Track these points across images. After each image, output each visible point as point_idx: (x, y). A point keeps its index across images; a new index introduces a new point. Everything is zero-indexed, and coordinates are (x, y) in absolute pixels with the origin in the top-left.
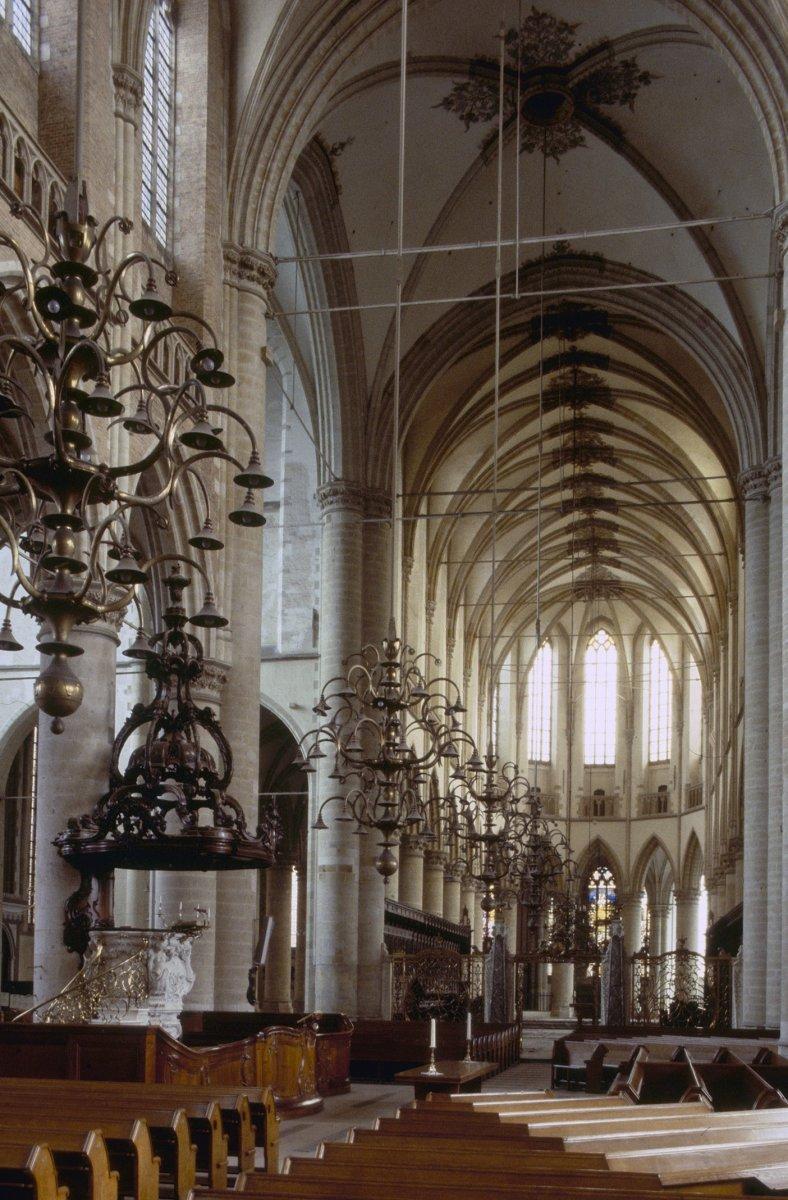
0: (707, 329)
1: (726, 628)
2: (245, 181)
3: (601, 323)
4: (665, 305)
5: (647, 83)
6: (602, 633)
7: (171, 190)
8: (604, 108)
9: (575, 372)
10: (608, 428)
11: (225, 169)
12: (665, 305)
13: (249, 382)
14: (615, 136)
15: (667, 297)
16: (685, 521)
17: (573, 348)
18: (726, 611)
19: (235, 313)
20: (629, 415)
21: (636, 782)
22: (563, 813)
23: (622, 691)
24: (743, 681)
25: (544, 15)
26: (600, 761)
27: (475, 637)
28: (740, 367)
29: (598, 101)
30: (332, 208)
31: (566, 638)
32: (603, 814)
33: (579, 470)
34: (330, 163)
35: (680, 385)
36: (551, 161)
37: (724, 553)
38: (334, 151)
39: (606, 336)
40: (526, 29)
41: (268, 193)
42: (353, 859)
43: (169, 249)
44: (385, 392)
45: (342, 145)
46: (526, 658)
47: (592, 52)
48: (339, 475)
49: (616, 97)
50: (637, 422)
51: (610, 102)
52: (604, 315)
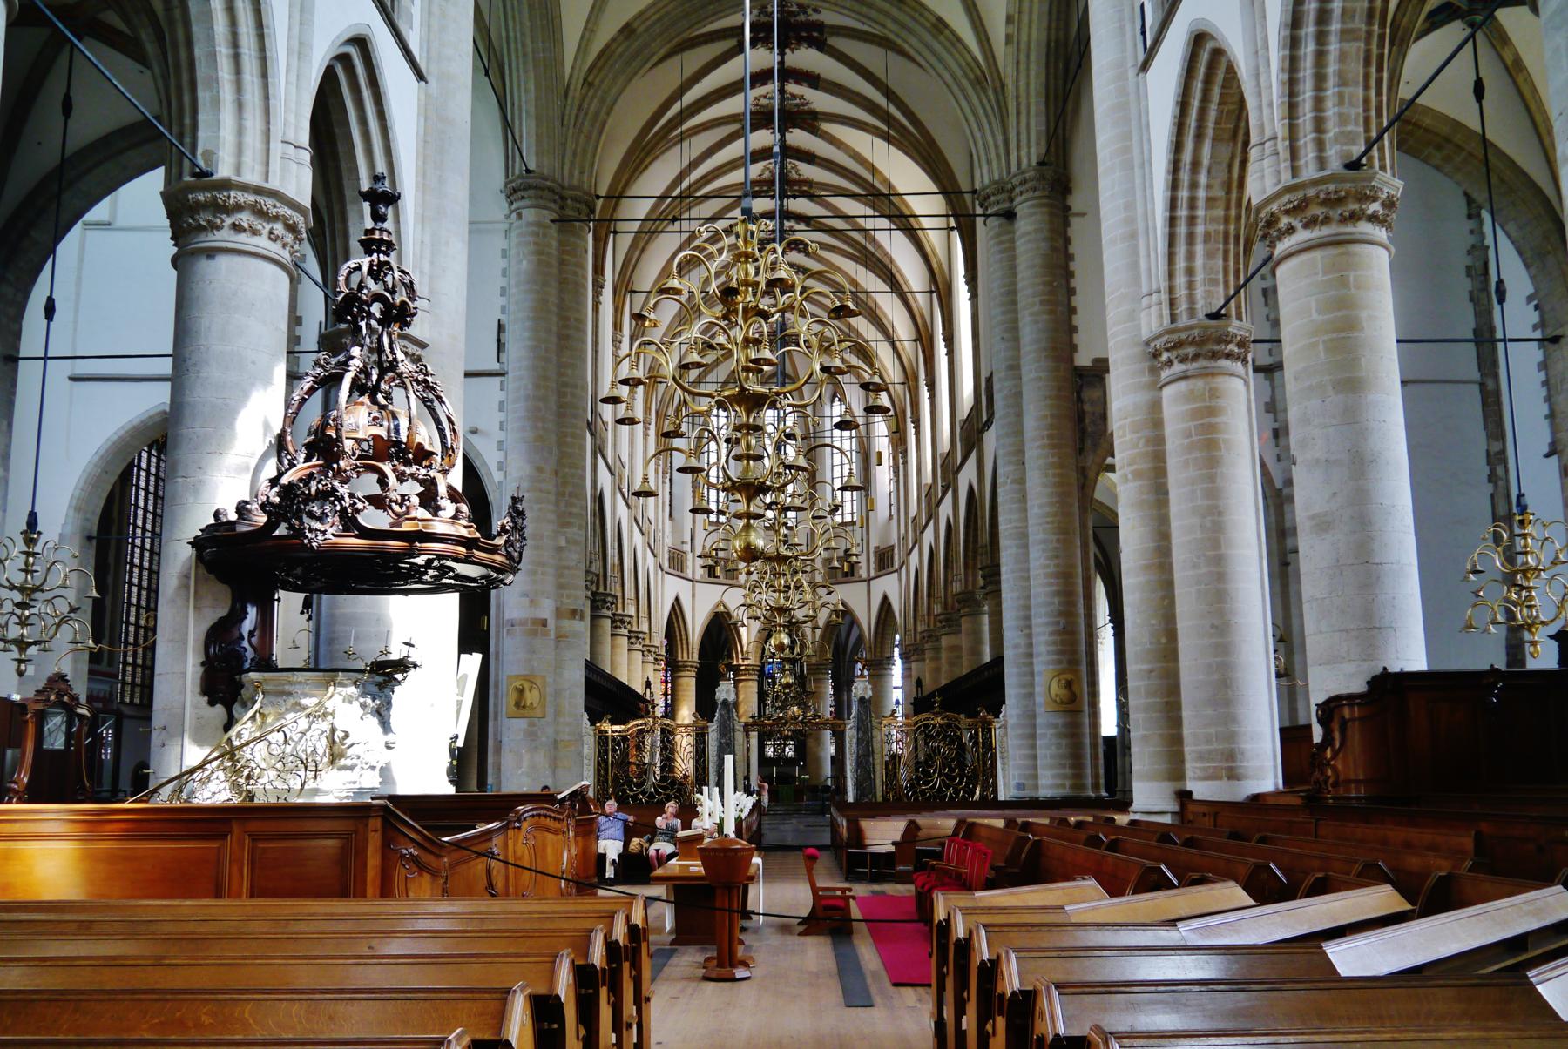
39: (820, 49)
42: (546, 610)
44: (585, 80)
52: (820, 26)
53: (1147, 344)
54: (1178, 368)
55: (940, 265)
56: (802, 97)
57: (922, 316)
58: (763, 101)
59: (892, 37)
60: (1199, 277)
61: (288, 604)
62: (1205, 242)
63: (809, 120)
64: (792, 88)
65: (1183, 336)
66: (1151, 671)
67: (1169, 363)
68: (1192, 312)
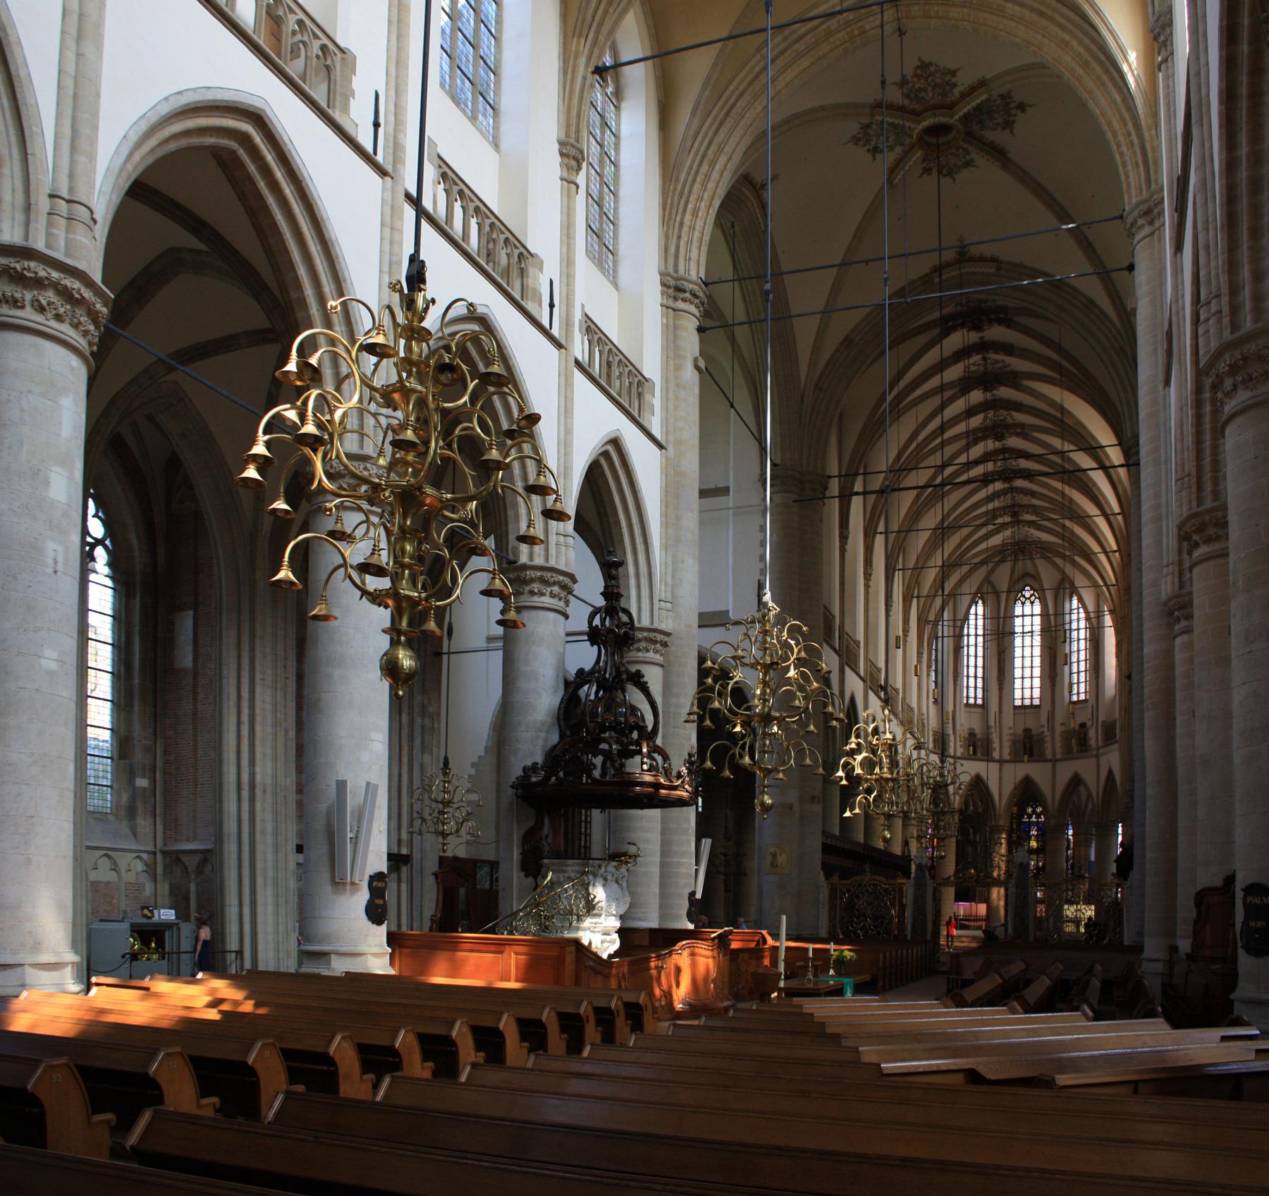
3: (1003, 316)
5: (1024, 111)
8: (989, 135)
9: (984, 359)
10: (1019, 407)
14: (999, 154)
17: (981, 338)
25: (930, 64)
26: (1027, 702)
33: (998, 445)
36: (946, 182)
40: (916, 75)
47: (973, 89)
49: (998, 124)
55: (1125, 490)
57: (1120, 529)
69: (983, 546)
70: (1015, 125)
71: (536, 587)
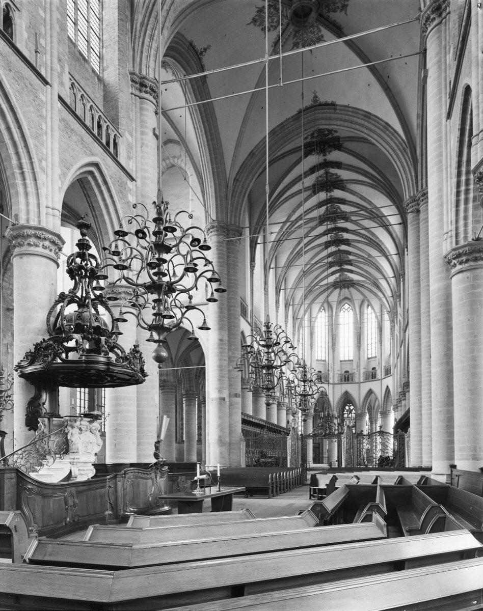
0: (388, 132)
1: (400, 291)
2: (141, 40)
4: (366, 124)
6: (346, 305)
7: (101, 44)
9: (327, 173)
11: (130, 33)
12: (366, 124)
13: (147, 146)
15: (367, 119)
16: (380, 244)
17: (325, 160)
18: (400, 284)
19: (138, 110)
20: (353, 193)
21: (363, 364)
22: (331, 381)
23: (355, 328)
24: (408, 310)
26: (347, 359)
27: (290, 305)
28: (404, 149)
29: (329, 11)
30: (203, 85)
31: (330, 306)
32: (348, 381)
33: (333, 226)
34: (200, 60)
35: (375, 171)
37: (398, 254)
38: (201, 53)
39: (340, 150)
41: (153, 47)
42: (225, 394)
43: (101, 75)
45: (205, 50)
46: (314, 315)
48: (215, 219)
50: (357, 196)
51: (335, 12)
53: (445, 257)
54: (459, 267)
56: (336, 174)
58: (320, 179)
59: (366, 136)
60: (470, 220)
61: (64, 391)
62: (474, 201)
63: (339, 184)
64: (333, 171)
65: (461, 251)
66: (441, 411)
67: (455, 265)
68: (466, 238)
69: (325, 282)
70: (348, 8)
71: (32, 240)
